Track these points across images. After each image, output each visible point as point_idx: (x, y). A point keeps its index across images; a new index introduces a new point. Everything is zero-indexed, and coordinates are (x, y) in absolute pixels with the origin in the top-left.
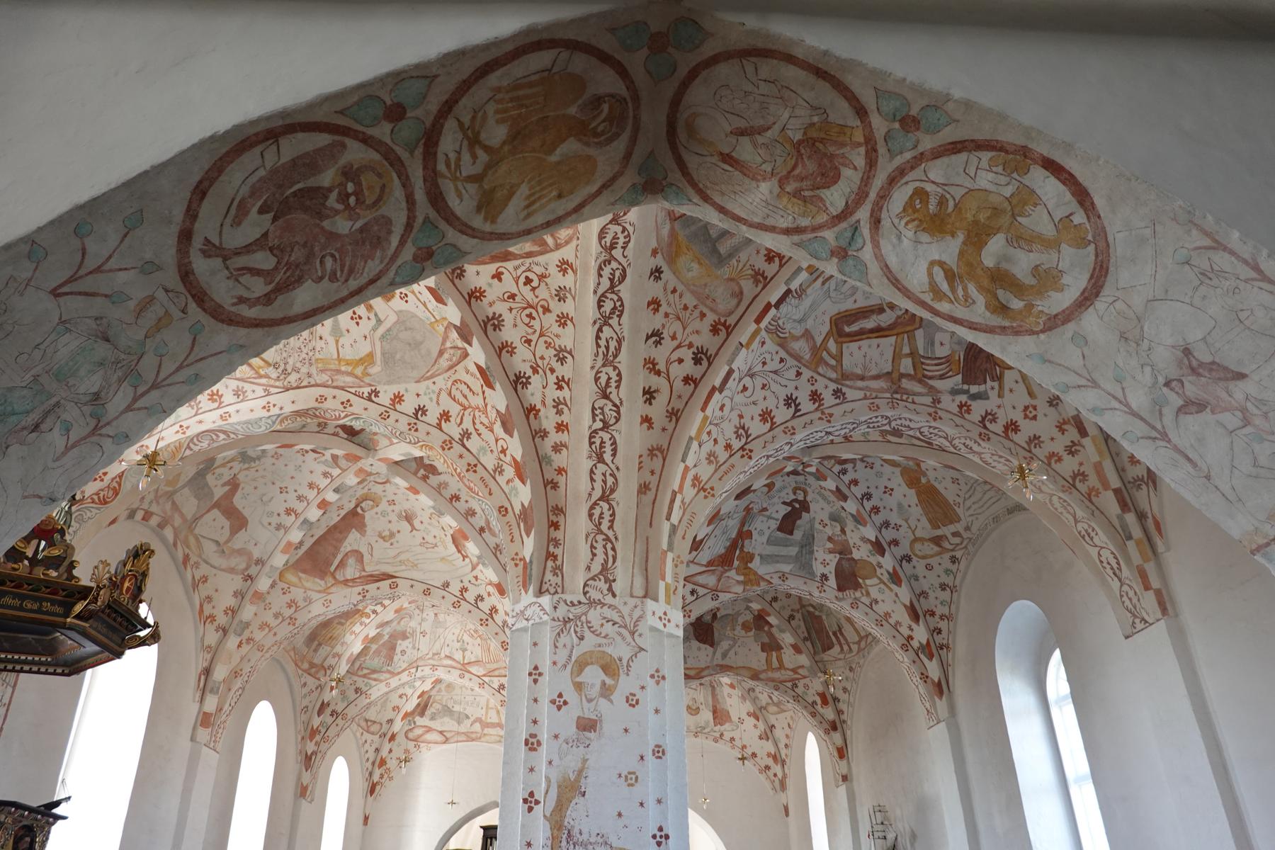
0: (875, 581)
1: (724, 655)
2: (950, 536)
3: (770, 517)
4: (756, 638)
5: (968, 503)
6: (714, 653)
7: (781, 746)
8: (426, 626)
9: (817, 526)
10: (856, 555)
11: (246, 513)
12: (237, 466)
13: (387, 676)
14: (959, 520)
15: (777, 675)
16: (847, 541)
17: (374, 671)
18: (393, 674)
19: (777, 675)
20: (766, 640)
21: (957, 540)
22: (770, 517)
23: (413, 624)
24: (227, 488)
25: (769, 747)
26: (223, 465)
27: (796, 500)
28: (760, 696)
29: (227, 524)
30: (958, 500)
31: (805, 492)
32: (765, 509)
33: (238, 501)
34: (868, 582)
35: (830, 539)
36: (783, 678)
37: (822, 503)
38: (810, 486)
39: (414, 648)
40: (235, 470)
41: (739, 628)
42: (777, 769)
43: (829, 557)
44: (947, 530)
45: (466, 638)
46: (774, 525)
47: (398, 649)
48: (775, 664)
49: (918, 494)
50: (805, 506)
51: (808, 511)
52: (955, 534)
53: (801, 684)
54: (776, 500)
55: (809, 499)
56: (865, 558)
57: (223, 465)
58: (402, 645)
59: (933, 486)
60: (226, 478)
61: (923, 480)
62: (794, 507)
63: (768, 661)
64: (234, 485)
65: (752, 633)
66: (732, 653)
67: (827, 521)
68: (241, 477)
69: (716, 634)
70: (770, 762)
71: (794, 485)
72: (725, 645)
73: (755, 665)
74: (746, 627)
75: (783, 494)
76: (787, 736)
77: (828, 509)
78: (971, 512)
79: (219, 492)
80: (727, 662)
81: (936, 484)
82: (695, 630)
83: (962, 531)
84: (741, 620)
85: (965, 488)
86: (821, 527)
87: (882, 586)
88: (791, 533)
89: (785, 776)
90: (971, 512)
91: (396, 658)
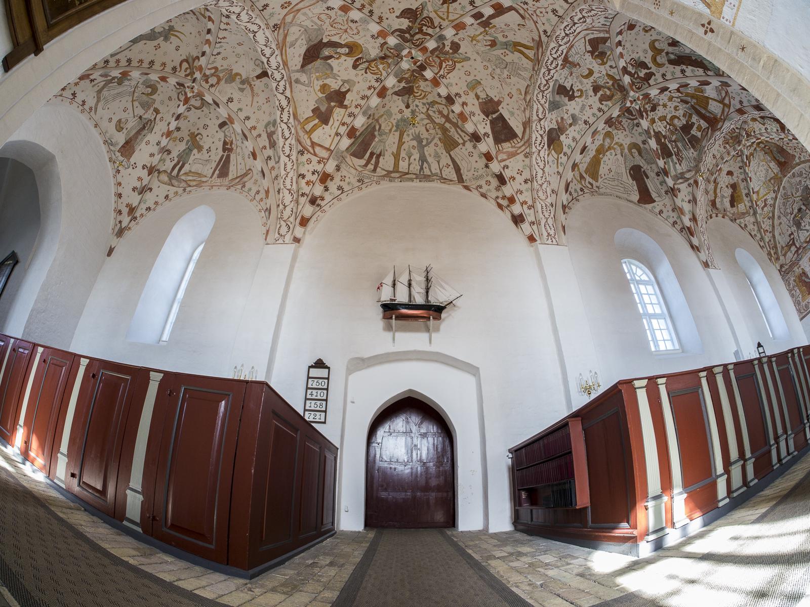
0: (556, 156)
1: (297, 81)
2: (587, 181)
3: (566, 78)
4: (319, 101)
5: (606, 181)
6: (297, 71)
7: (144, 206)
9: (565, 108)
10: (563, 138)
14: (597, 181)
15: (301, 133)
16: (567, 129)
19: (301, 133)
20: (323, 108)
21: (590, 186)
22: (566, 78)
25: (135, 199)
27: (573, 92)
28: (168, 161)
30: (603, 175)
31: (580, 96)
32: (571, 74)
34: (553, 152)
35: (562, 118)
36: (302, 140)
37: (578, 108)
41: (320, 83)
42: (126, 220)
43: (554, 122)
44: (588, 179)
46: (561, 82)
48: (308, 127)
49: (594, 156)
50: (572, 98)
51: (570, 100)
52: (589, 183)
55: (576, 99)
59: (600, 161)
61: (601, 156)
62: (570, 91)
63: (308, 120)
65: (321, 95)
66: (299, 86)
69: (310, 66)
70: (125, 211)
71: (584, 89)
72: (304, 78)
73: (299, 111)
74: (324, 87)
75: (578, 84)
76: (156, 203)
77: (577, 112)
78: (604, 184)
81: (602, 162)
82: (315, 45)
83: (594, 186)
84: (328, 81)
85: (610, 176)
86: (565, 111)
88: (557, 94)
89: (128, 228)
90: (604, 184)
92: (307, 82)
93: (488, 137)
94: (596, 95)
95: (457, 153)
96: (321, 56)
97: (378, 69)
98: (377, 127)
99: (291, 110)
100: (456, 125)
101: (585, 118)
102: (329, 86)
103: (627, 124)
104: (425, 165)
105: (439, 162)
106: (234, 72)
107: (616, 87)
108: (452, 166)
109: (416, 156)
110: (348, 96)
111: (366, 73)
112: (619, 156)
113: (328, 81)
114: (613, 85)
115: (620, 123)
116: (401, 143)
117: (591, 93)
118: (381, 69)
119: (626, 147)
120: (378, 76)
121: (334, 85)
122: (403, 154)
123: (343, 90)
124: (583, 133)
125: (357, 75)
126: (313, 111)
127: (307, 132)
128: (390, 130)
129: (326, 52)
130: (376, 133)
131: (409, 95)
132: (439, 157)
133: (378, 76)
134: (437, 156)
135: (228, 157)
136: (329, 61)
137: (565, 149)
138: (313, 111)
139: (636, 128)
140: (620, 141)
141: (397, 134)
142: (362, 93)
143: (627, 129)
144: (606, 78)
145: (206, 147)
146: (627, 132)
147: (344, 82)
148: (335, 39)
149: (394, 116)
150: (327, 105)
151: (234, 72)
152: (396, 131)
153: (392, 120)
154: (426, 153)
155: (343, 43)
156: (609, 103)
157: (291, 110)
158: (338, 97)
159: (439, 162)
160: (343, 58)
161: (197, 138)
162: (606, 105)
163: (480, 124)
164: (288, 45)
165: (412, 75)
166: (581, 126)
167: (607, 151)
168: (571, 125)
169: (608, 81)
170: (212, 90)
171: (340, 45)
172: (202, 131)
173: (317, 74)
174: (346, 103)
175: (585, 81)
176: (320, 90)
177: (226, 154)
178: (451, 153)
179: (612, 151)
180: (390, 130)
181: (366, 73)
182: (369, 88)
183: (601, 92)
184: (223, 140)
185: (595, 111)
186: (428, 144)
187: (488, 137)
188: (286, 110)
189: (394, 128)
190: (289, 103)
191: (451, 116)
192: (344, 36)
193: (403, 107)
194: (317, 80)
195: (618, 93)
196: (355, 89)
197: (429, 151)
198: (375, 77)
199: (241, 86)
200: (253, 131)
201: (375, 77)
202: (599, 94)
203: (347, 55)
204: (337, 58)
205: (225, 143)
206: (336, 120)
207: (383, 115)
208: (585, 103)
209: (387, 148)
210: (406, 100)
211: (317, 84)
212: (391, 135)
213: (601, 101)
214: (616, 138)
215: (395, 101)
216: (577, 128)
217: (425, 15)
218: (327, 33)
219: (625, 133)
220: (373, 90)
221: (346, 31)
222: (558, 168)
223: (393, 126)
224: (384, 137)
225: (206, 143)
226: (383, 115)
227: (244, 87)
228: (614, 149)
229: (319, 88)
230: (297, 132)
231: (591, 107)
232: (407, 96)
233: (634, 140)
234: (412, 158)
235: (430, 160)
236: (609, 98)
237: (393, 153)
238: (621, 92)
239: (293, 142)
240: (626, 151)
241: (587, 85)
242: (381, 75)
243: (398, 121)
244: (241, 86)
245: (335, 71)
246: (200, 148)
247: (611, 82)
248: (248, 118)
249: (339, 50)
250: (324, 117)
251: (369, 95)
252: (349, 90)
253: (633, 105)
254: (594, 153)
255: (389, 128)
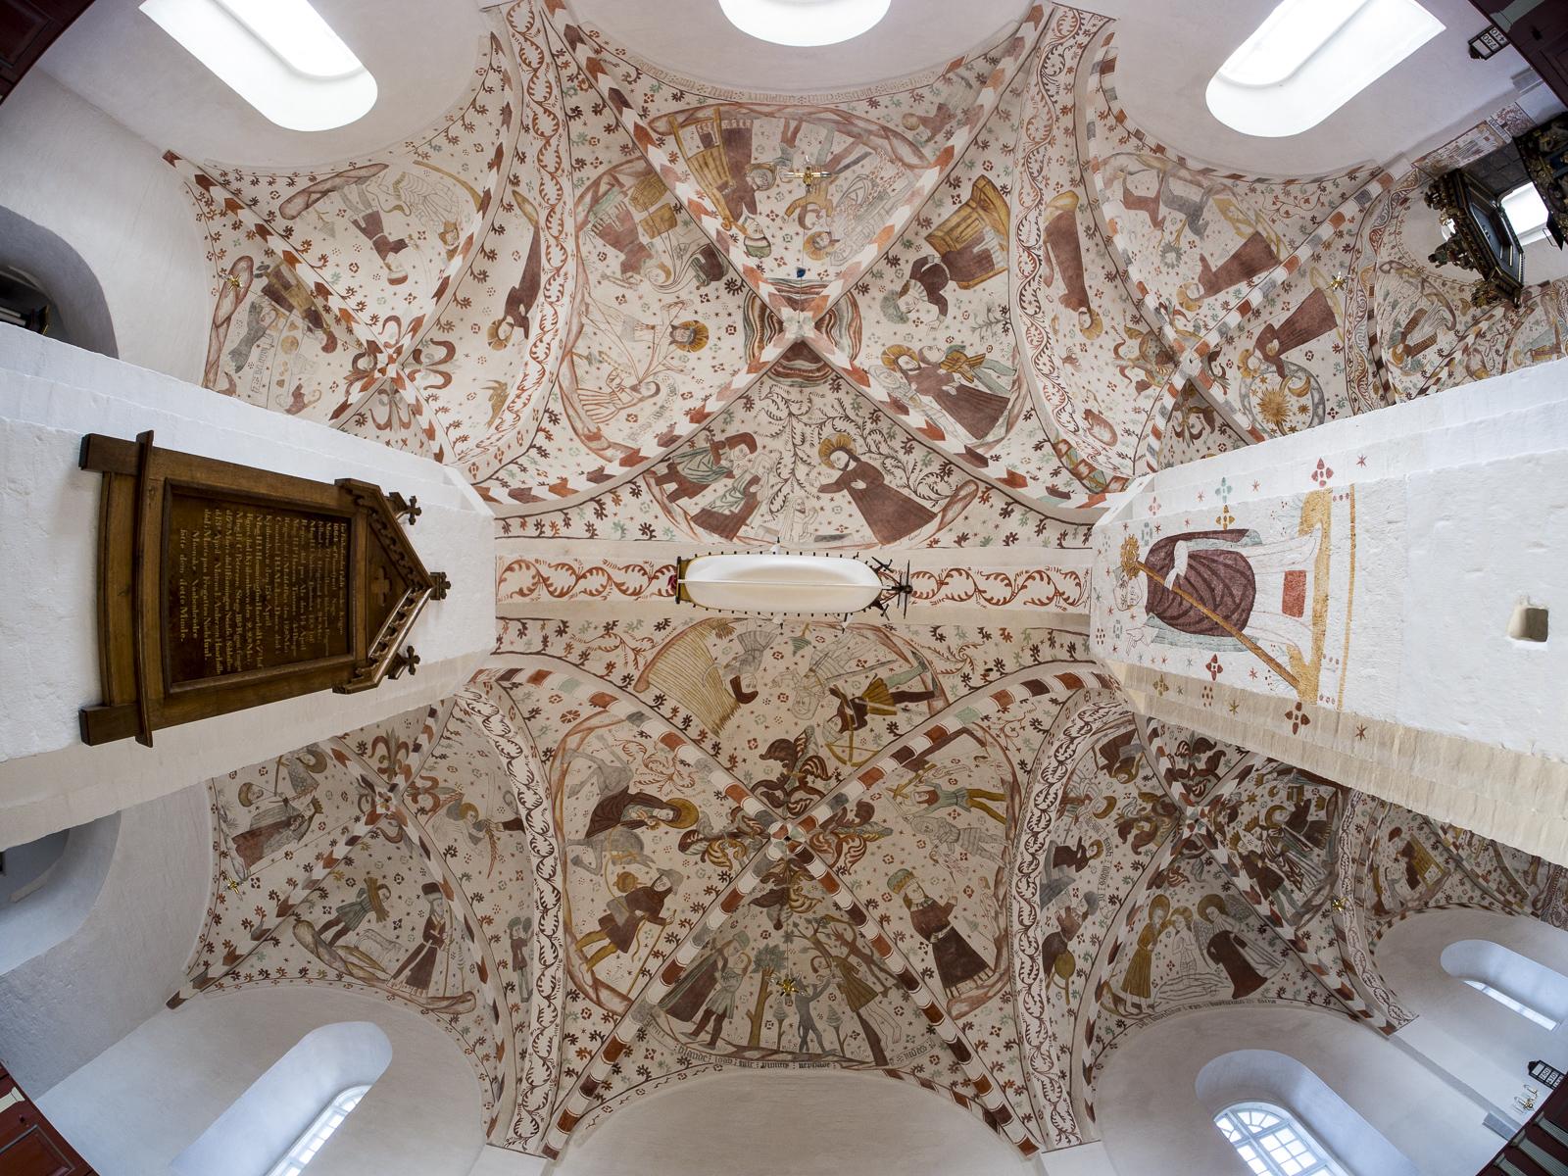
0: (1062, 982)
1: (577, 861)
6: (579, 843)
8: (633, 308)
9: (1070, 887)
10: (1073, 945)
11: (1132, 212)
12: (1169, 238)
13: (581, 218)
15: (576, 961)
17: (596, 201)
18: (579, 228)
19: (576, 961)
22: (1068, 831)
23: (645, 287)
24: (1160, 218)
26: (1180, 232)
29: (1137, 193)
32: (1077, 819)
33: (1144, 215)
34: (1057, 978)
35: (1068, 909)
37: (1095, 879)
38: (1110, 853)
39: (604, 276)
40: (1167, 234)
41: (619, 870)
43: (1054, 922)
45: (606, 369)
46: (1060, 842)
47: (610, 251)
49: (1137, 954)
50: (1081, 863)
53: (582, 1003)
54: (1085, 827)
56: (1076, 956)
57: (1180, 232)
58: (616, 258)
60: (1167, 223)
61: (1149, 947)
63: (590, 937)
64: (1158, 224)
65: (618, 893)
66: (579, 870)
67: (1081, 894)
68: (1158, 233)
69: (601, 836)
72: (589, 856)
74: (624, 879)
75: (1091, 833)
77: (1093, 888)
79: (1163, 211)
80: (571, 867)
81: (1153, 957)
82: (614, 797)
84: (633, 868)
86: (1072, 893)
87: (1063, 992)
91: (599, 242)
92: (594, 866)
93: (931, 976)
94: (1125, 840)
95: (873, 1011)
96: (623, 819)
97: (725, 855)
98: (720, 965)
99: (560, 914)
100: (869, 960)
101: (1111, 892)
102: (635, 879)
103: (1189, 868)
104: (811, 1035)
105: (837, 1029)
106: (465, 800)
107: (1160, 811)
108: (863, 1035)
109: (793, 1018)
110: (668, 901)
111: (703, 860)
112: (1185, 933)
113: (633, 868)
114: (1154, 809)
115: (1176, 872)
116: (764, 994)
117: (1116, 840)
118: (731, 856)
119: (1194, 909)
120: (725, 869)
121: (644, 877)
122: (768, 1015)
123: (660, 888)
124: (1109, 922)
125: (686, 863)
126: (601, 921)
127: (586, 960)
128: (745, 970)
129: (634, 813)
130: (718, 975)
131: (782, 905)
132: (838, 1019)
133: (725, 869)
134: (835, 1020)
135: (432, 953)
136: (638, 831)
137: (1080, 964)
138: (601, 921)
139: (1206, 868)
140: (1183, 904)
141: (758, 977)
142: (694, 900)
143: (1191, 877)
144: (1140, 801)
145: (393, 916)
146: (1193, 883)
147: (662, 873)
148: (651, 790)
149: (752, 944)
150: (627, 914)
151: (465, 800)
152: (755, 971)
153: (748, 950)
154: (813, 1014)
155: (665, 799)
156: (1152, 846)
157: (560, 914)
158: (650, 901)
159: (837, 1029)
160: (663, 827)
161: (380, 892)
162: (1146, 854)
163: (915, 954)
164: (566, 791)
165: (787, 868)
166: (1105, 911)
167: (1160, 933)
168: (1085, 916)
169: (1144, 805)
170: (423, 818)
171: (661, 805)
172: (392, 885)
173: (615, 853)
174: (663, 914)
175: (1102, 822)
176: (617, 884)
177: (428, 945)
178: (862, 1011)
179: (1171, 929)
180: (745, 970)
181: (703, 860)
182: (708, 891)
183: (1135, 832)
184: (427, 916)
185: (1128, 871)
186: (816, 995)
187: (931, 976)
188: (552, 913)
189: (753, 966)
190: (558, 900)
191: (860, 943)
192: (667, 787)
193: (769, 926)
194: (614, 863)
195: (1166, 820)
196: (682, 889)
197: (818, 1009)
198: (720, 870)
199: (474, 832)
200: (485, 925)
201: (720, 870)
202: (1131, 838)
203: (671, 822)
204: (653, 828)
205: (430, 925)
206: (642, 944)
207: (730, 942)
208: (1107, 864)
209: (738, 1002)
210: (775, 915)
211: (613, 872)
212: (746, 978)
213: (1135, 848)
214: (1174, 905)
215: (754, 917)
216: (1098, 916)
217: (811, 753)
218: (636, 778)
219: (1188, 886)
220: (714, 894)
221: (670, 778)
222: (1068, 1003)
223: (750, 961)
224: (733, 982)
225: (396, 909)
226: (730, 942)
227: (481, 835)
228: (1173, 923)
229: (615, 879)
230: (568, 957)
231: (1118, 867)
232: (778, 906)
233: (1207, 891)
234: (786, 1023)
235: (820, 1025)
236: (1149, 837)
237: (748, 1013)
238: (1169, 815)
239: (560, 974)
240: (1196, 916)
241: (1109, 827)
242: (731, 868)
243: (760, 952)
244: (474, 832)
245: (647, 851)
246: (382, 915)
247: (1149, 806)
248: (479, 898)
249: (656, 812)
250: (621, 937)
251: (706, 904)
252: (669, 890)
253: (1196, 831)
254: (1136, 947)
255: (743, 966)
